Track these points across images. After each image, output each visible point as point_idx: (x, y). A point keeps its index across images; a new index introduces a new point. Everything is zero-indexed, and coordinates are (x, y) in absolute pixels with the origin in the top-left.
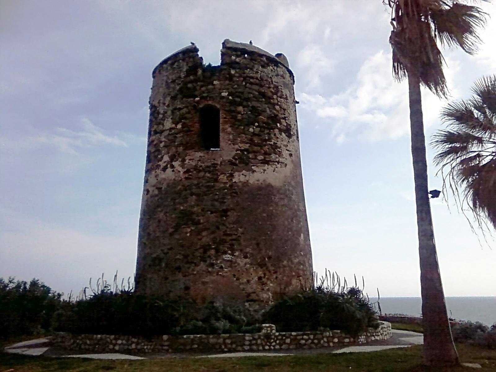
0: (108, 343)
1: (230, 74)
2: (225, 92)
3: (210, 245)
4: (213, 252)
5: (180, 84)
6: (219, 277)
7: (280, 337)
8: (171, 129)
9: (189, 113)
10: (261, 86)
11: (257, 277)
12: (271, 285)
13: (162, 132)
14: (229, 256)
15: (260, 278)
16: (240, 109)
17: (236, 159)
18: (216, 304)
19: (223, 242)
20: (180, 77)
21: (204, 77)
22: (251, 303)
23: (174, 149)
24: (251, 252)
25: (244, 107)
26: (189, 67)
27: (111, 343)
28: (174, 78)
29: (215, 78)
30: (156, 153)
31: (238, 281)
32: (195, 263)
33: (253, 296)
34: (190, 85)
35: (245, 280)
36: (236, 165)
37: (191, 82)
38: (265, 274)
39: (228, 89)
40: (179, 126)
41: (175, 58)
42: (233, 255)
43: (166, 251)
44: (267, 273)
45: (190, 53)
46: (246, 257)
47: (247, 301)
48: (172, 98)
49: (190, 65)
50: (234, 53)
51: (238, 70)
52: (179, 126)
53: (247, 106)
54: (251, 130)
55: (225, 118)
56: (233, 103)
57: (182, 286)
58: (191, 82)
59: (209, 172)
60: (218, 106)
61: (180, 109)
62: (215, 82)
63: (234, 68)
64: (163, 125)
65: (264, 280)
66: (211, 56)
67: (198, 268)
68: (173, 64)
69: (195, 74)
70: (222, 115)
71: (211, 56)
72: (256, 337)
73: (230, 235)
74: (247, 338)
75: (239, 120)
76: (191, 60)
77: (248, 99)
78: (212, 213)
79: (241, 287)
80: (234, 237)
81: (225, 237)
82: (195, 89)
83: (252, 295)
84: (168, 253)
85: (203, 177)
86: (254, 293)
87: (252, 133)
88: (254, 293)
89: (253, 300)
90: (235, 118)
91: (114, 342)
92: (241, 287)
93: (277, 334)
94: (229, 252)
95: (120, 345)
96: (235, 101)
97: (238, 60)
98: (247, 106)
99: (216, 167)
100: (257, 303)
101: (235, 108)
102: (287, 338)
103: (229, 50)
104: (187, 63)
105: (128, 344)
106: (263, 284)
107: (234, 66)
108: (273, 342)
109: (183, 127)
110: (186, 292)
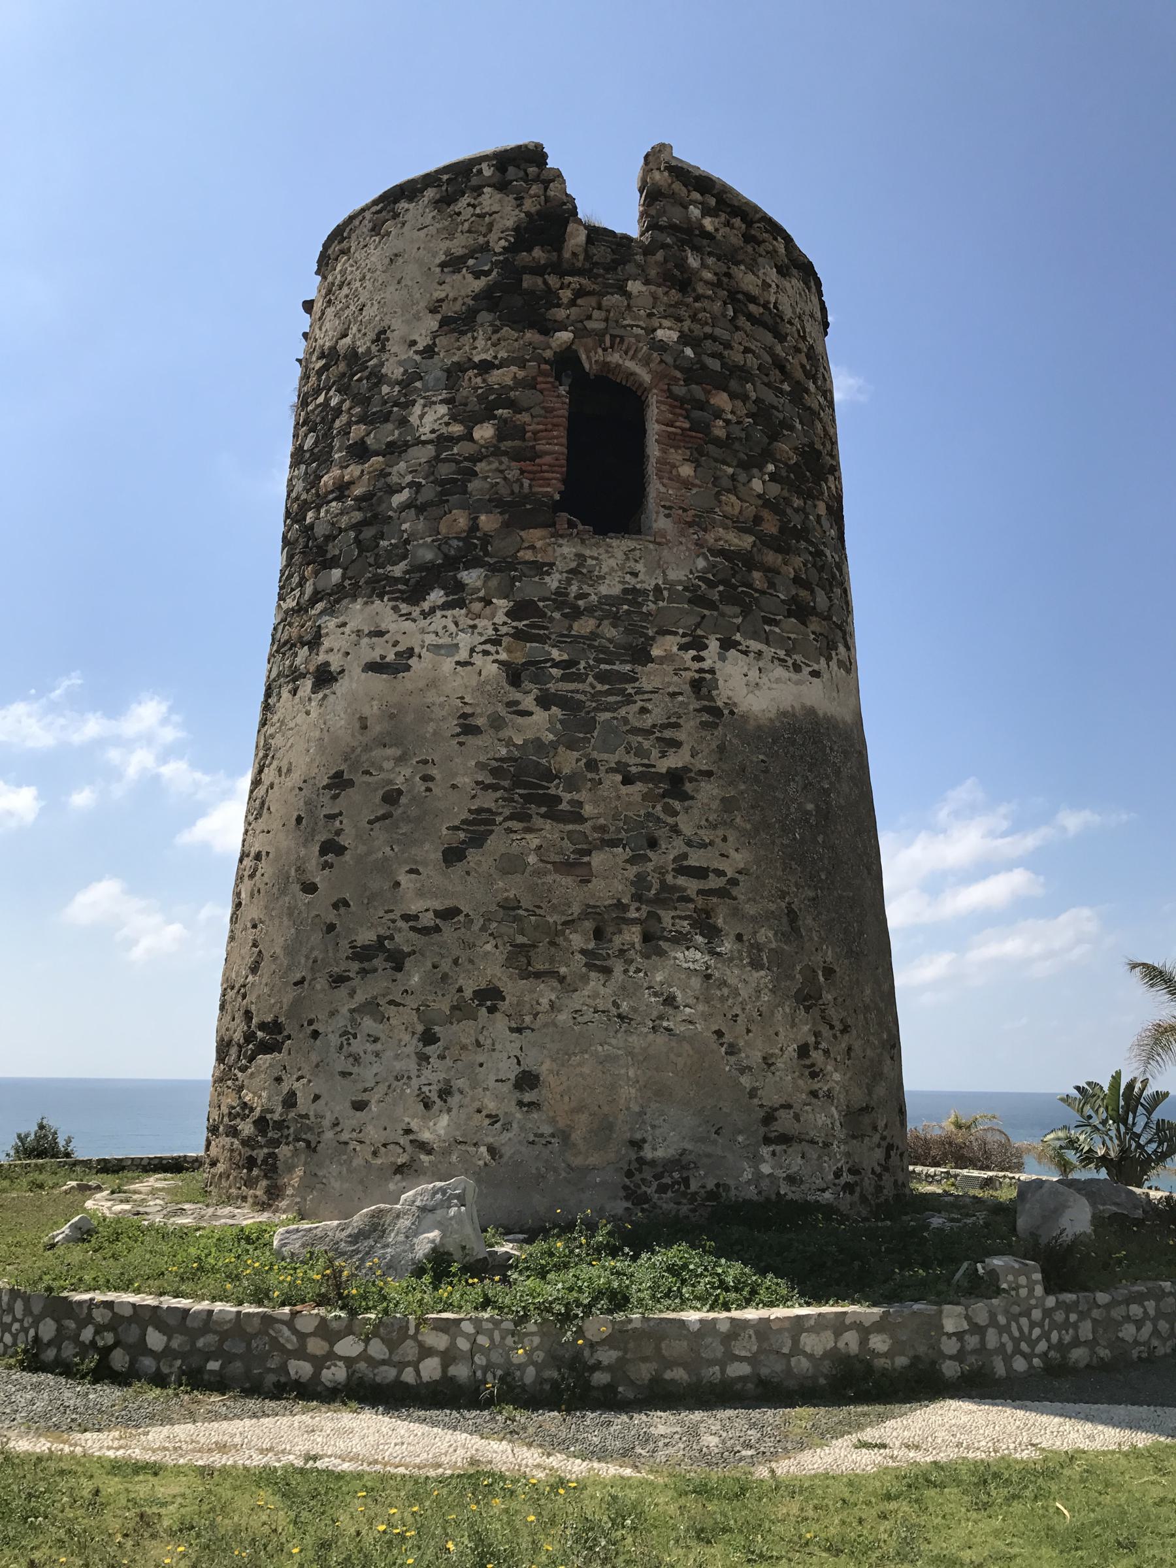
0: (282, 1349)
1: (682, 265)
2: (670, 329)
3: (623, 907)
4: (632, 935)
5: (487, 273)
6: (661, 1039)
7: (1059, 1316)
8: (443, 441)
9: (529, 384)
10: (781, 338)
11: (795, 1046)
12: (837, 1076)
13: (394, 450)
14: (698, 955)
15: (803, 1051)
16: (721, 400)
17: (711, 585)
18: (654, 1149)
19: (669, 896)
20: (485, 248)
21: (588, 257)
22: (778, 1148)
23: (462, 520)
24: (774, 945)
25: (733, 396)
26: (528, 214)
27: (301, 1353)
28: (460, 252)
29: (630, 268)
30: (368, 533)
31: (732, 1059)
32: (562, 979)
33: (784, 1124)
34: (528, 281)
35: (756, 1057)
36: (712, 605)
37: (538, 270)
38: (817, 1034)
39: (679, 319)
40: (484, 432)
41: (453, 183)
42: (712, 953)
43: (427, 920)
44: (826, 1032)
45: (523, 165)
46: (756, 965)
47: (767, 1141)
48: (444, 322)
49: (529, 205)
50: (696, 196)
51: (710, 261)
52: (484, 432)
53: (745, 398)
54: (757, 485)
55: (670, 424)
56: (694, 373)
57: (510, 1071)
58: (538, 270)
59: (616, 620)
60: (647, 378)
61: (485, 367)
62: (634, 286)
63: (696, 249)
64: (404, 422)
65: (816, 1056)
66: (609, 200)
67: (577, 1000)
68: (445, 202)
69: (556, 241)
70: (654, 411)
71: (609, 200)
72: (982, 1319)
73: (700, 873)
74: (949, 1326)
75: (717, 442)
76: (535, 189)
77: (743, 373)
78: (628, 780)
79: (746, 1081)
80: (714, 882)
81: (681, 881)
82: (550, 298)
83: (782, 1114)
84: (437, 929)
85: (594, 635)
86: (788, 1106)
87: (759, 496)
88: (788, 1106)
89: (785, 1139)
90: (706, 429)
91: (316, 1346)
92: (746, 1081)
93: (1051, 1301)
94: (699, 939)
95: (349, 1361)
96: (704, 367)
97: (708, 223)
98: (745, 398)
99: (641, 605)
100: (796, 1147)
101: (709, 392)
102: (1083, 1316)
103: (673, 185)
104: (519, 199)
105: (396, 1358)
106: (813, 1075)
107: (698, 241)
108: (1039, 1339)
109: (501, 435)
110: (528, 1097)
